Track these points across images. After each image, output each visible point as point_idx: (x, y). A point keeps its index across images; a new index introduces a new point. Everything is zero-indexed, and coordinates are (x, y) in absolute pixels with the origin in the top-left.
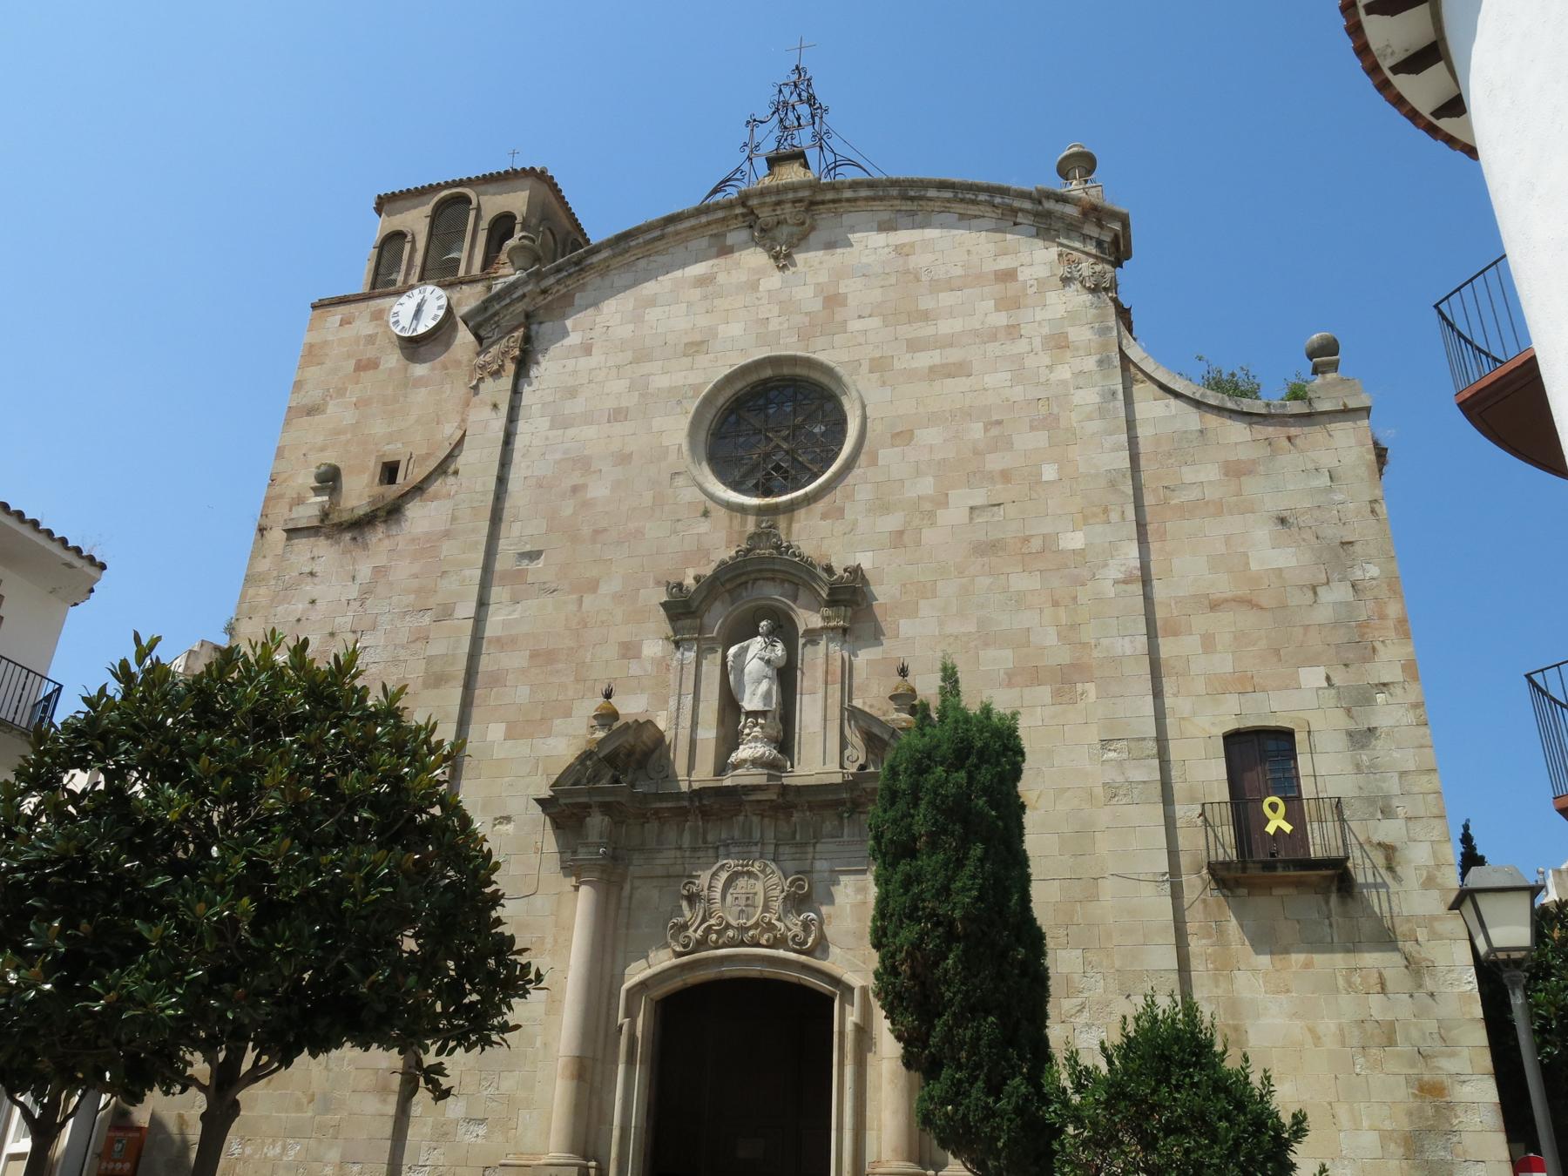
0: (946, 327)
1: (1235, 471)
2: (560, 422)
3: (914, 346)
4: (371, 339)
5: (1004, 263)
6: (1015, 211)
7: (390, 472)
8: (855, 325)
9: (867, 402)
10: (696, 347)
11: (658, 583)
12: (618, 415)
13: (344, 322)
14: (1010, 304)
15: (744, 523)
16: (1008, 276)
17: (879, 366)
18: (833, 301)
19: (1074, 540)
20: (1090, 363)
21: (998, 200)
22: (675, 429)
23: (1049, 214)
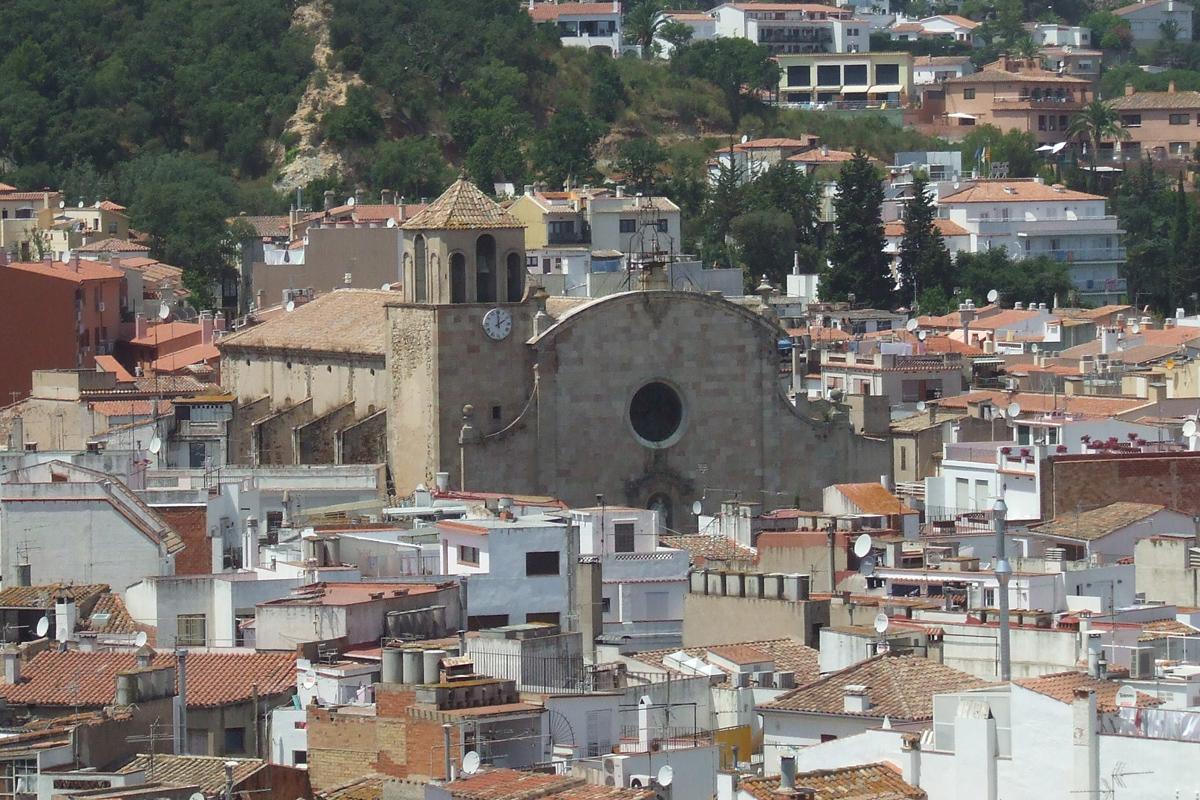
0: (720, 371)
1: (809, 448)
2: (575, 399)
3: (710, 378)
4: (473, 333)
5: (741, 342)
6: (746, 317)
7: (496, 412)
8: (686, 364)
9: (693, 406)
10: (626, 366)
11: (622, 480)
12: (598, 398)
13: (457, 320)
14: (742, 362)
15: (650, 455)
16: (742, 349)
17: (696, 386)
18: (678, 350)
19: (758, 472)
20: (768, 399)
21: (742, 312)
22: (621, 408)
23: (759, 324)
